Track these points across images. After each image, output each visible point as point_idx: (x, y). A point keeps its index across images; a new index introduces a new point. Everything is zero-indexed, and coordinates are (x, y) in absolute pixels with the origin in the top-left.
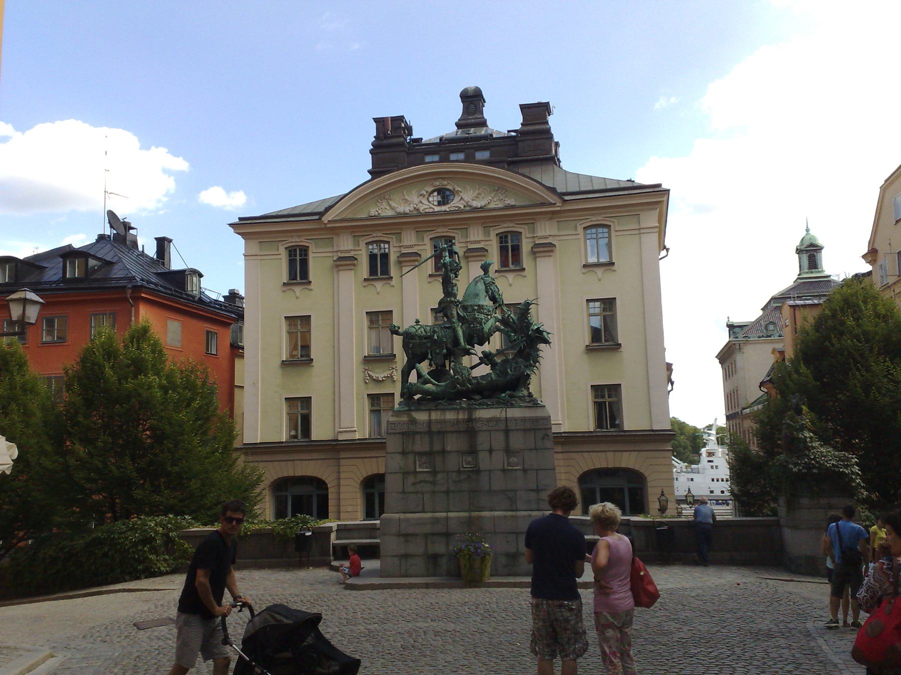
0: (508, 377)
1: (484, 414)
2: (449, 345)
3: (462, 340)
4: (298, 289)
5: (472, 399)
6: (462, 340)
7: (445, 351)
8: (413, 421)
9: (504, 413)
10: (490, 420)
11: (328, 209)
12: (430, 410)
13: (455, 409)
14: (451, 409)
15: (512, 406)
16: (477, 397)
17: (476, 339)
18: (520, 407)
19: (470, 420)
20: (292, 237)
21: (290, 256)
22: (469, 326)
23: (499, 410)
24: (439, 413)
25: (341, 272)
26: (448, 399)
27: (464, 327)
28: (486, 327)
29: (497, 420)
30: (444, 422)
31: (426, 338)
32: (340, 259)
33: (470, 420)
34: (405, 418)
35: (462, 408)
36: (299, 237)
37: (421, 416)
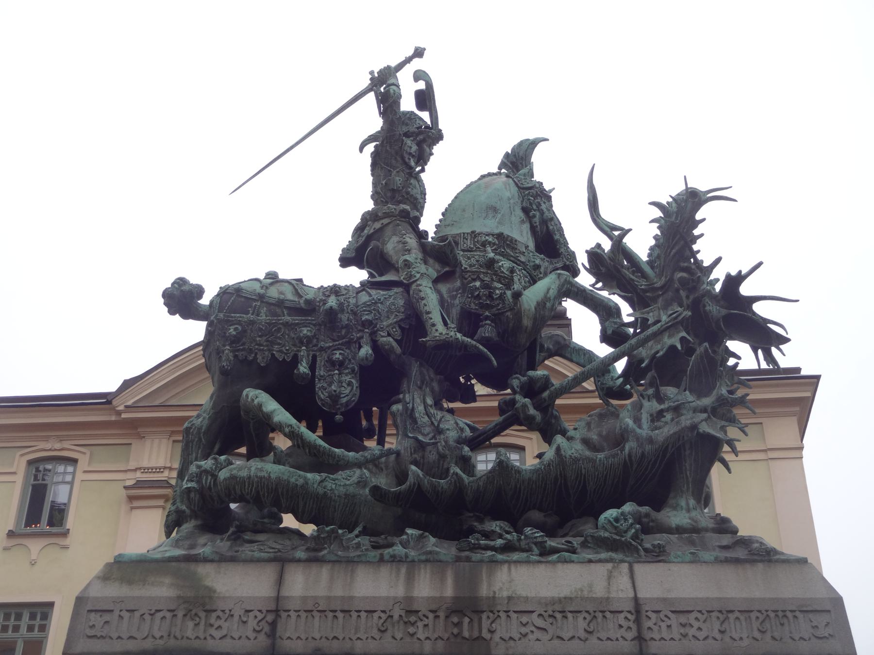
0: (630, 446)
1: (528, 580)
2: (384, 339)
3: (436, 317)
4: (35, 546)
5: (471, 531)
6: (436, 317)
7: (366, 351)
8: (200, 605)
9: (623, 581)
10: (559, 610)
11: (127, 384)
12: (281, 561)
13: (395, 560)
14: (381, 560)
15: (658, 555)
16: (495, 526)
17: (487, 330)
18: (695, 560)
19: (467, 607)
20: (46, 439)
21: (36, 478)
22: (464, 287)
23: (601, 570)
24: (325, 571)
25: (135, 512)
26: (365, 532)
27: (444, 288)
28: (532, 296)
29: (599, 611)
30: (345, 610)
31: (296, 310)
32: (139, 484)
33: (467, 607)
34: (162, 590)
35: (431, 560)
36: (61, 439)
37: (241, 584)
